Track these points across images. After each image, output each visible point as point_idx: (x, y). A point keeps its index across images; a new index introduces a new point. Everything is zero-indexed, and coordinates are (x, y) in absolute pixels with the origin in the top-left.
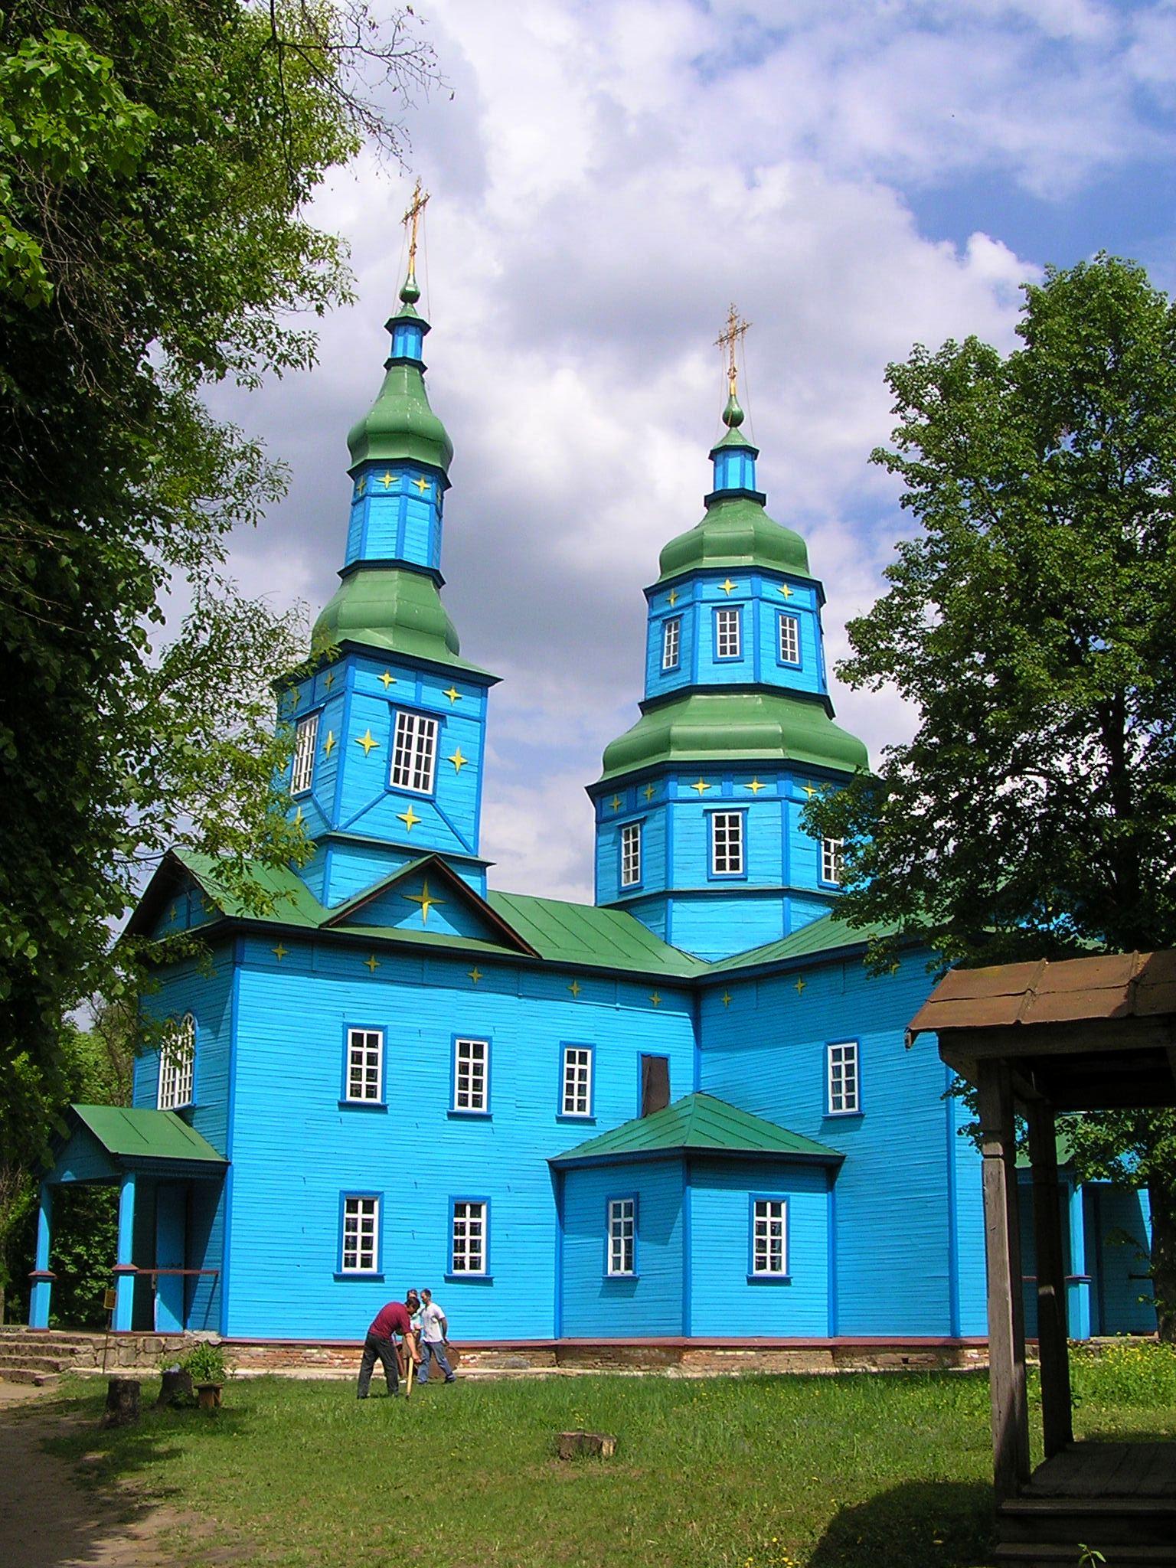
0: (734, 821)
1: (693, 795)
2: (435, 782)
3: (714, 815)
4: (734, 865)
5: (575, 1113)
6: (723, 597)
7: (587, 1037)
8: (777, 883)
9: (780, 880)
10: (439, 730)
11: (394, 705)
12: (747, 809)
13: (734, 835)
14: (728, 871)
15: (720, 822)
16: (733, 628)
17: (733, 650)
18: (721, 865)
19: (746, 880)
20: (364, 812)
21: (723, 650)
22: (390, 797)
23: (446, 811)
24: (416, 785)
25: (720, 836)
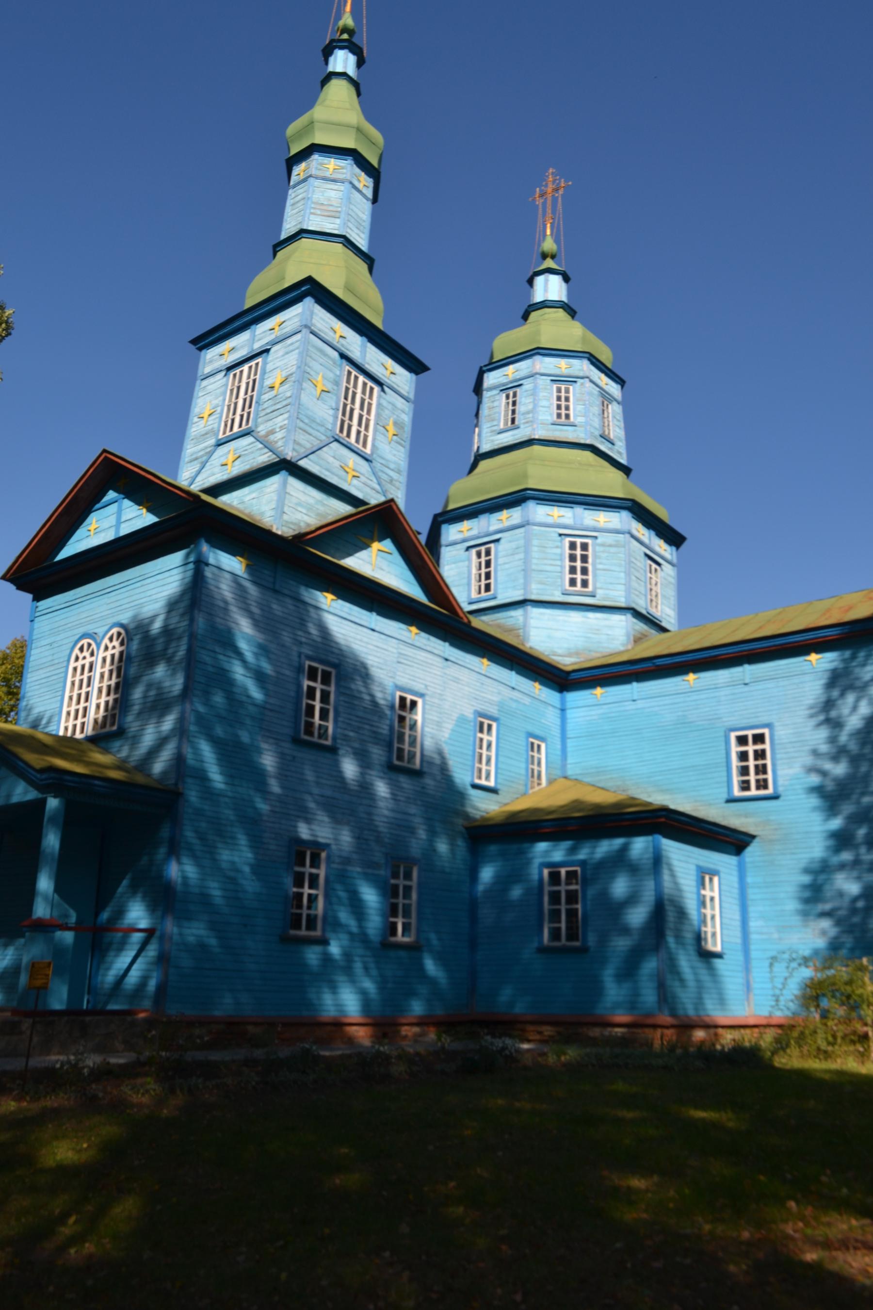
0: (585, 547)
1: (550, 520)
2: (373, 445)
3: (568, 539)
4: (585, 584)
5: (483, 782)
6: (557, 372)
7: (493, 711)
8: (622, 603)
9: (623, 600)
10: (379, 397)
11: (343, 356)
12: (596, 537)
13: (584, 559)
14: (579, 587)
15: (573, 546)
16: (567, 399)
17: (567, 416)
18: (573, 582)
19: (594, 596)
20: (313, 453)
21: (559, 416)
22: (335, 445)
23: (380, 474)
24: (357, 441)
25: (573, 558)
